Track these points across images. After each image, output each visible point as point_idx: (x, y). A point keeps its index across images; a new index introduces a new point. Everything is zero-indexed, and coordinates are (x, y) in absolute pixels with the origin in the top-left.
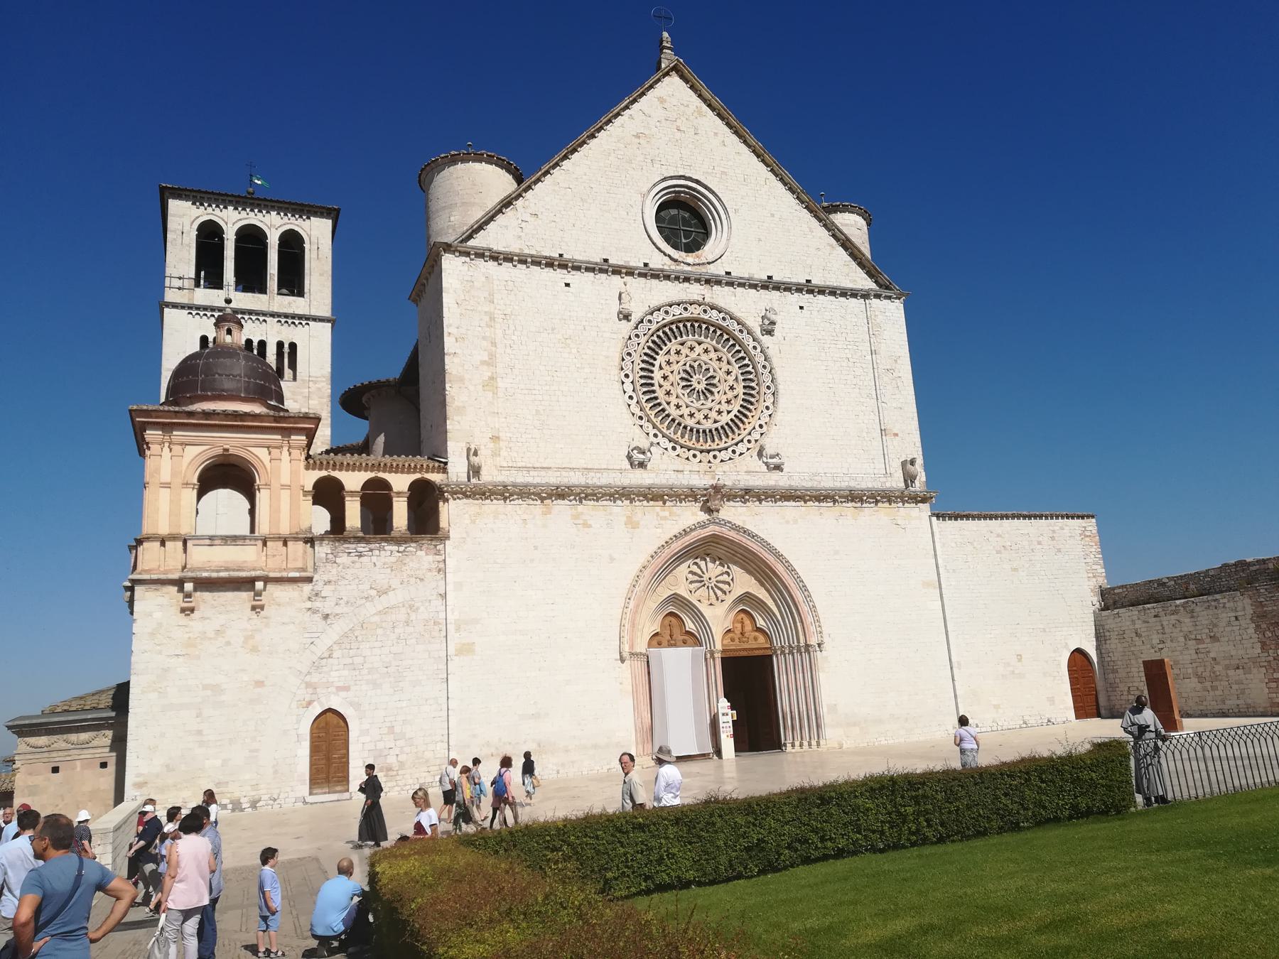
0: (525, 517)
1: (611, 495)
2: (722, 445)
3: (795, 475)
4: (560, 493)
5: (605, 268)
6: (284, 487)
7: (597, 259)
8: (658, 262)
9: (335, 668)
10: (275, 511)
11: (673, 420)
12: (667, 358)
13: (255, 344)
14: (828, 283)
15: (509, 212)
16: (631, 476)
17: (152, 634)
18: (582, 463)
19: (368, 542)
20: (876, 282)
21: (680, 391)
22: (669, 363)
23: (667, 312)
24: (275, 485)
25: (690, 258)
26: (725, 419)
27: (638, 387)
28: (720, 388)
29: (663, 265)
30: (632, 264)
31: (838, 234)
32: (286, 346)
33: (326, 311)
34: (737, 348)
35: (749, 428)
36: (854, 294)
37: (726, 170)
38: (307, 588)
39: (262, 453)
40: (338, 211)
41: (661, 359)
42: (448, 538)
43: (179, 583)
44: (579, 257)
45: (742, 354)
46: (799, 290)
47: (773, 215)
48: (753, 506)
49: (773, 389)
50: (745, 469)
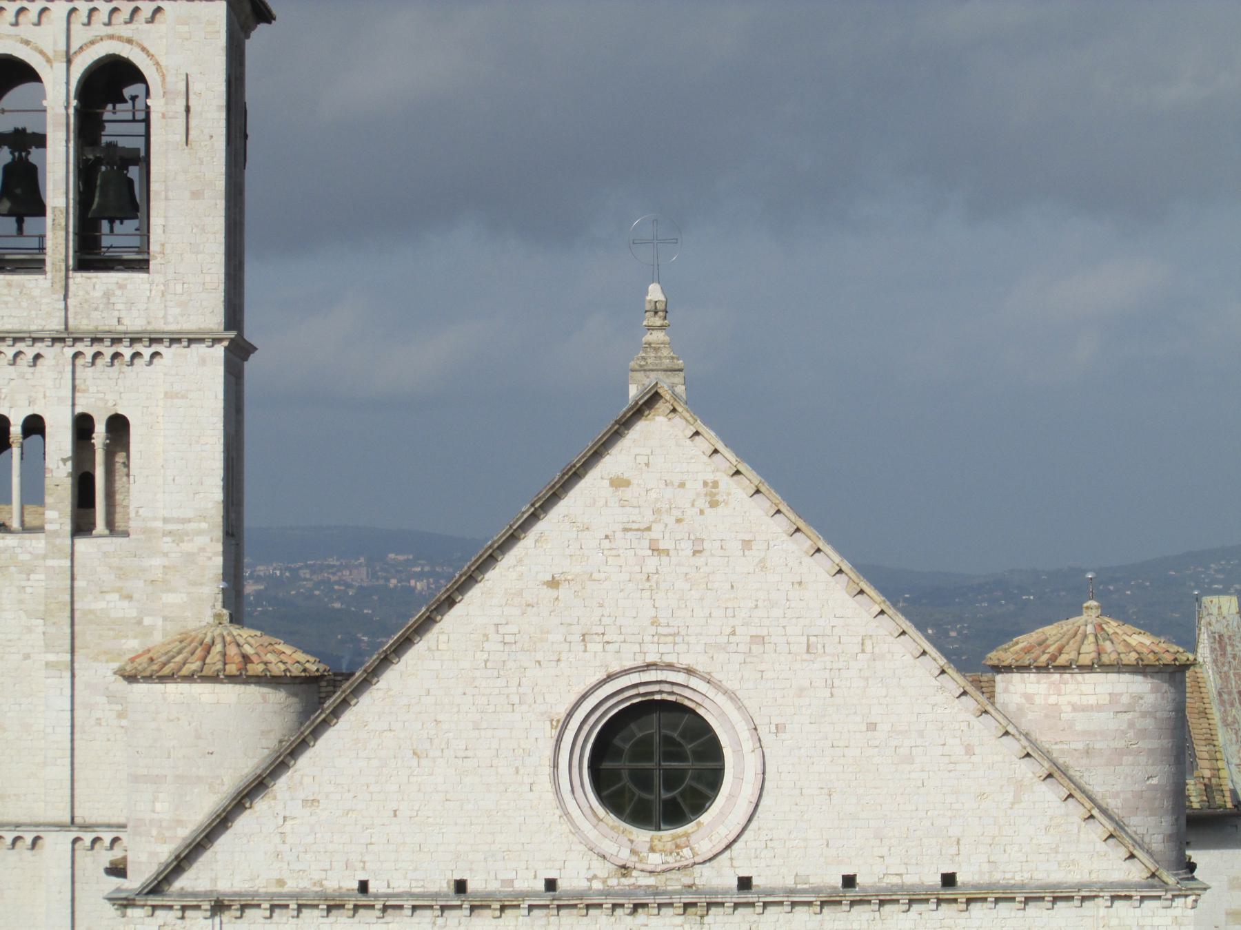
14: (998, 877)
15: (261, 805)
29: (589, 880)
30: (521, 885)
36: (1059, 896)
37: (764, 632)
44: (400, 886)
47: (872, 727)
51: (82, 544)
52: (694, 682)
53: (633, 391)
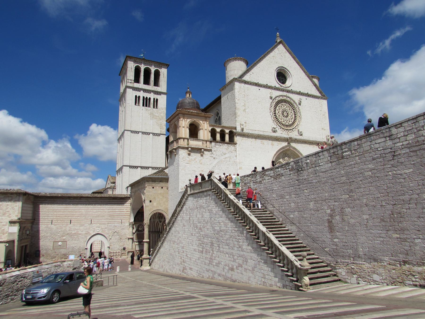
0: (251, 141)
1: (269, 138)
2: (290, 129)
3: (305, 137)
6: (206, 130)
7: (265, 84)
8: (278, 86)
9: (216, 169)
10: (204, 135)
11: (280, 122)
12: (279, 108)
13: (148, 98)
16: (272, 134)
17: (183, 158)
18: (262, 130)
19: (222, 143)
20: (321, 95)
21: (282, 116)
22: (279, 109)
23: (279, 97)
24: (204, 129)
25: (284, 85)
26: (291, 123)
27: (273, 114)
28: (290, 116)
30: (272, 86)
31: (314, 83)
32: (156, 99)
33: (165, 91)
34: (293, 107)
35: (295, 125)
38: (210, 152)
39: (201, 122)
40: (169, 65)
41: (277, 108)
42: (237, 144)
43: (187, 148)
45: (294, 108)
49: (300, 117)
50: (295, 134)
51: (154, 109)
52: (285, 70)
53: (278, 41)
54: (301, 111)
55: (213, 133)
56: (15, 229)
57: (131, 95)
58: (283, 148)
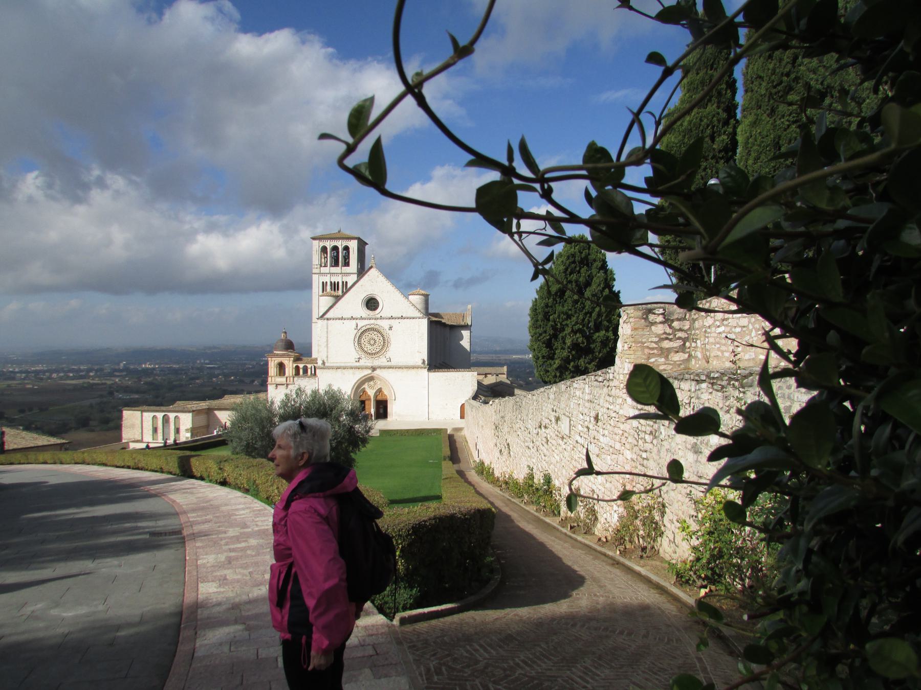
3: (393, 363)
4: (338, 368)
5: (352, 318)
7: (350, 317)
8: (364, 316)
26: (378, 350)
39: (286, 361)
46: (398, 318)
48: (383, 370)
54: (391, 337)
55: (297, 368)
56: (189, 435)
57: (317, 282)
58: (365, 376)
